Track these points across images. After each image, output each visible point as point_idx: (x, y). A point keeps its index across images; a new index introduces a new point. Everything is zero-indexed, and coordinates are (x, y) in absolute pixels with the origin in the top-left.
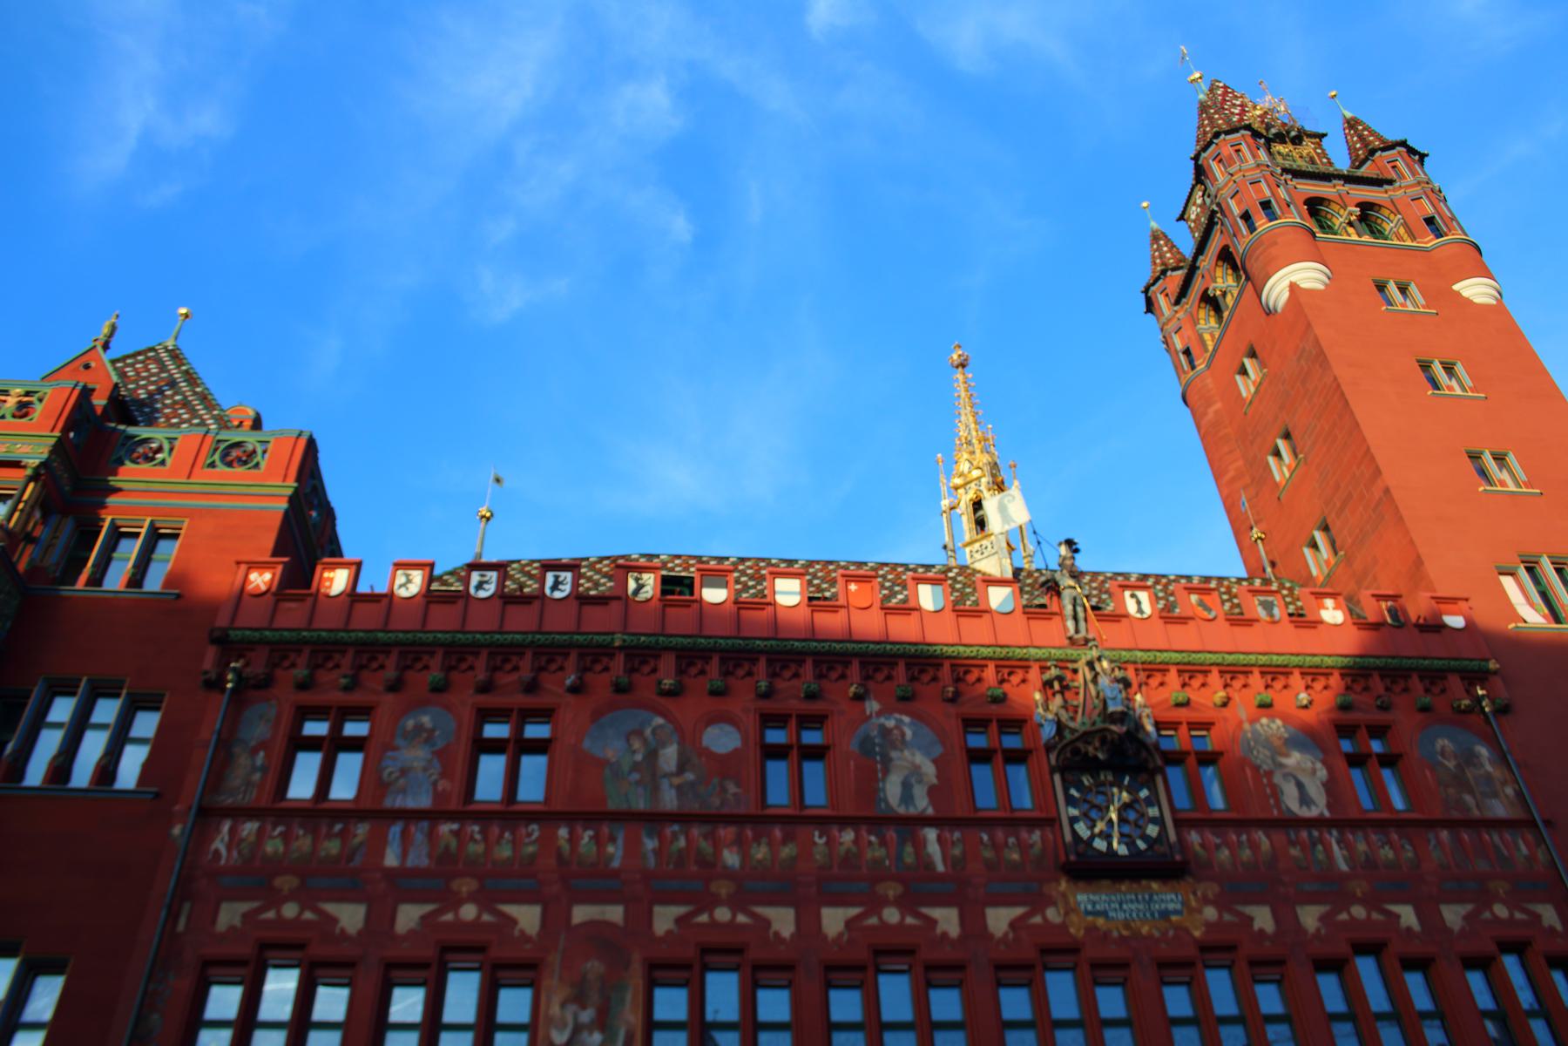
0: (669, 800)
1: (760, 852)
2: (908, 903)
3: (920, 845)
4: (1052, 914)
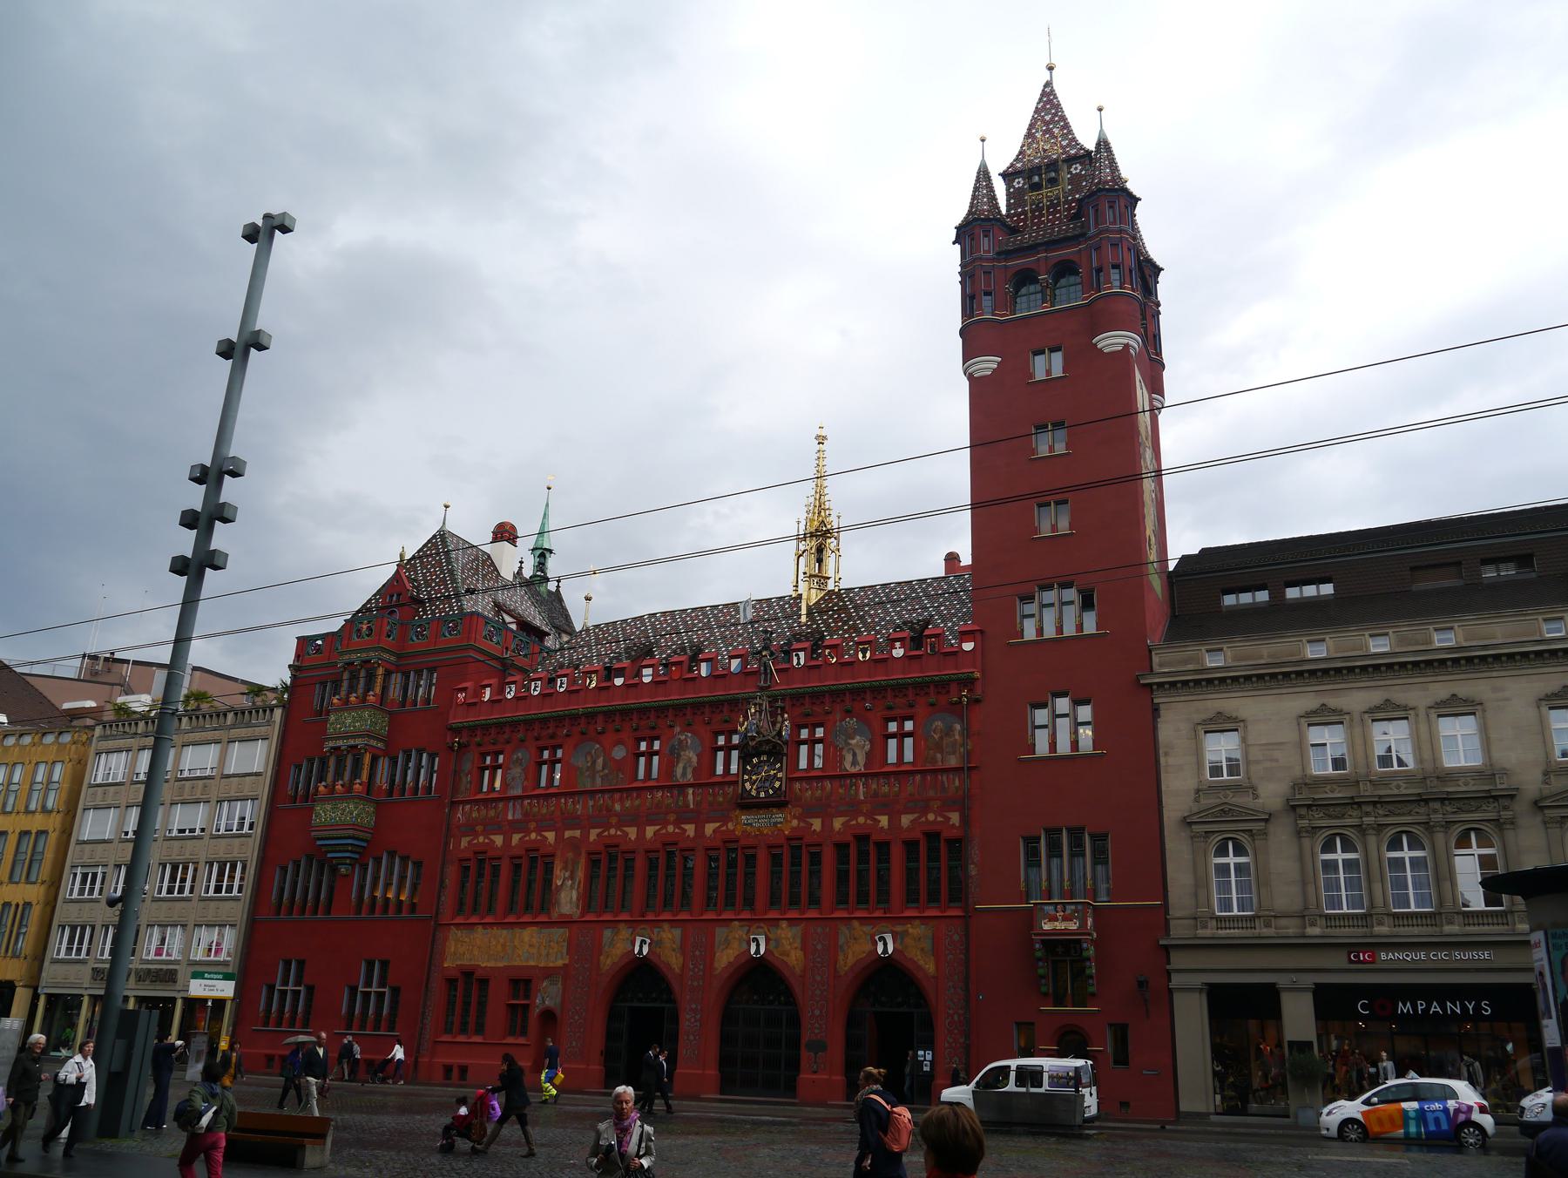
0: (599, 784)
1: (628, 804)
2: (677, 823)
3: (685, 796)
4: (731, 826)
